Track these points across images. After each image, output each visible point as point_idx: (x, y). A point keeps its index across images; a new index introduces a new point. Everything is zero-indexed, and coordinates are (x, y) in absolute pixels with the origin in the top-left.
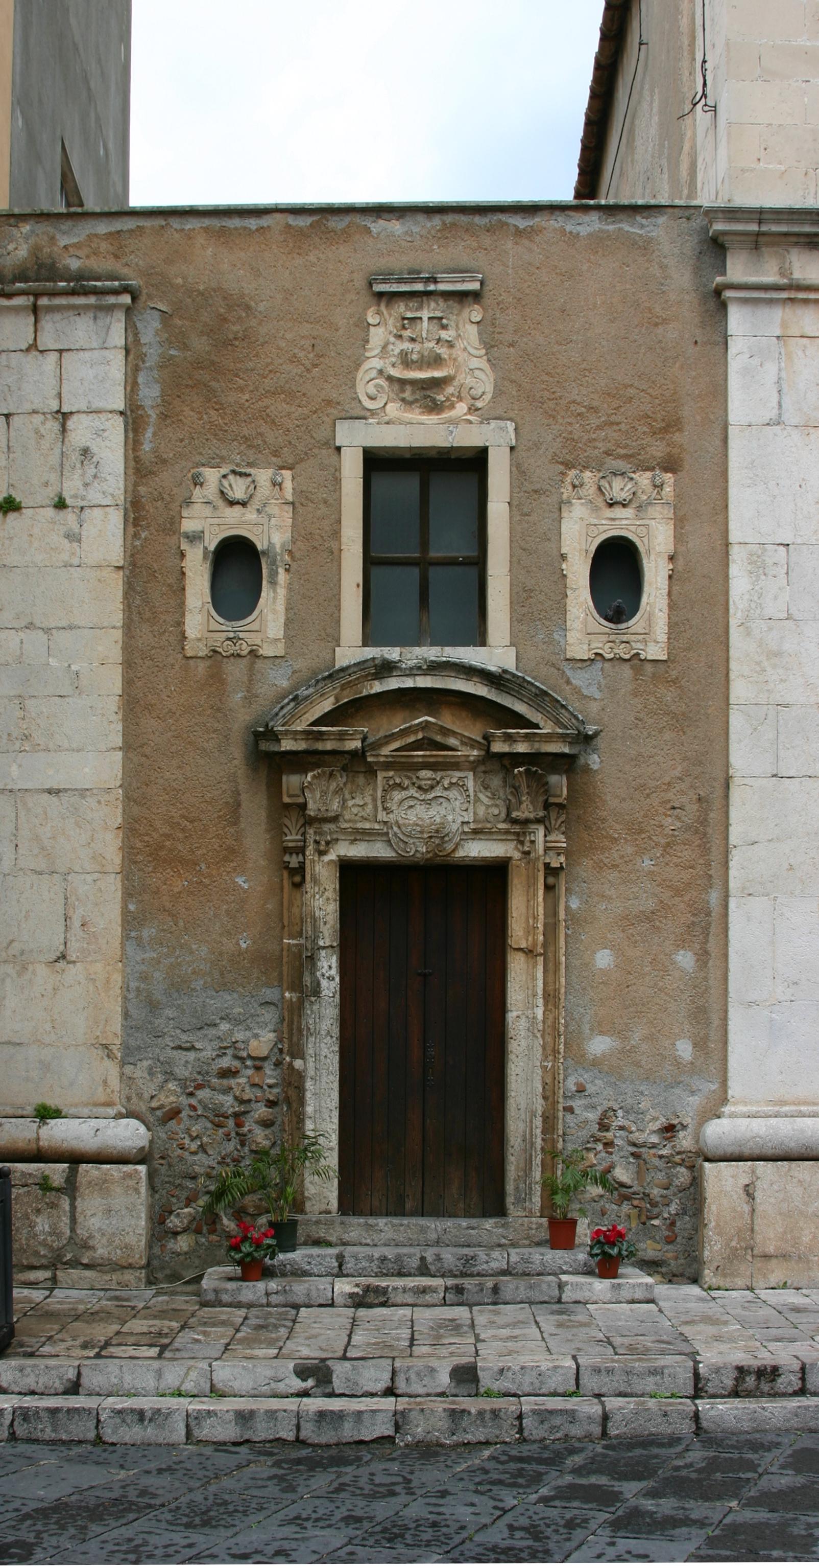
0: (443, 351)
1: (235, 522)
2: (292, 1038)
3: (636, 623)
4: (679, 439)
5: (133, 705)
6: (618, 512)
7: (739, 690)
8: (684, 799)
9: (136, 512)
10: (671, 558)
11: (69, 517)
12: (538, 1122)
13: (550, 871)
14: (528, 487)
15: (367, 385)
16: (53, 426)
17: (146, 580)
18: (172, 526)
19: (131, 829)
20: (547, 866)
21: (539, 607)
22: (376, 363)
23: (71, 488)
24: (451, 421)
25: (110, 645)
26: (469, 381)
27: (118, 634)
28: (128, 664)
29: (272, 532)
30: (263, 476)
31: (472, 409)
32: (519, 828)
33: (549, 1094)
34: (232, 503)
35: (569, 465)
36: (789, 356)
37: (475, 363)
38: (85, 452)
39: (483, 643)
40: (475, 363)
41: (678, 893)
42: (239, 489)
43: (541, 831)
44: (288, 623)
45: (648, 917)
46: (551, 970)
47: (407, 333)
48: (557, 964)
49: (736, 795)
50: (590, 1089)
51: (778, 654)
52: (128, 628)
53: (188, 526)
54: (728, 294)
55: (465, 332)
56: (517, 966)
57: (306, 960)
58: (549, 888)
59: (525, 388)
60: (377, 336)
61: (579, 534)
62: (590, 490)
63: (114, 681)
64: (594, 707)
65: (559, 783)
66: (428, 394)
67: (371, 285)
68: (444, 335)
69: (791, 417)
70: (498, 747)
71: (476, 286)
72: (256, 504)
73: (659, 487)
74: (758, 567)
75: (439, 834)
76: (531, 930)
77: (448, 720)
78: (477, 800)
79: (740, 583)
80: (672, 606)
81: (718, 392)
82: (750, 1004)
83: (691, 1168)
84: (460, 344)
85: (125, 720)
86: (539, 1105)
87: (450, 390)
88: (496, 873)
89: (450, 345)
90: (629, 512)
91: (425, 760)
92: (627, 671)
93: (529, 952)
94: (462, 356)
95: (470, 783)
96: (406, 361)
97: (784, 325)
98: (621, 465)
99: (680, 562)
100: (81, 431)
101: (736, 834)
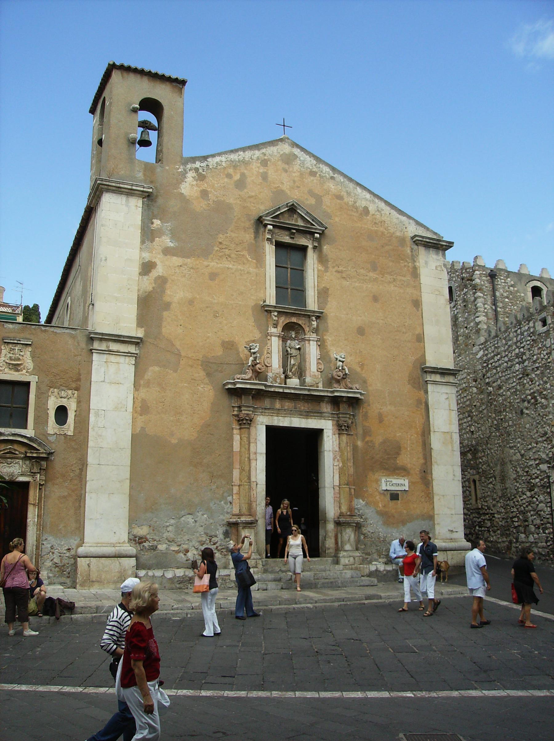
0: (21, 357)
6: (63, 399)
7: (91, 444)
8: (76, 469)
10: (75, 411)
12: (35, 547)
13: (40, 485)
14: (40, 391)
20: (40, 484)
21: (41, 420)
22: (3, 359)
24: (21, 374)
26: (27, 365)
31: (27, 372)
32: (33, 474)
33: (38, 540)
36: (108, 366)
37: (29, 361)
39: (26, 428)
40: (29, 361)
41: (73, 491)
43: (39, 475)
45: (65, 497)
47: (12, 352)
48: (41, 508)
49: (89, 468)
50: (49, 539)
51: (101, 436)
54: (93, 351)
55: (27, 354)
58: (40, 489)
60: (4, 352)
61: (52, 404)
62: (56, 394)
64: (54, 446)
65: (44, 463)
66: (16, 368)
67: (3, 340)
68: (21, 353)
69: (107, 381)
70: (28, 455)
71: (30, 343)
73: (74, 394)
74: (97, 415)
75: (12, 475)
76: (35, 499)
77: (16, 447)
78: (22, 466)
79: (92, 418)
81: (90, 373)
82: (91, 519)
83: (74, 559)
84: (25, 356)
86: (35, 543)
87: (22, 367)
89: (23, 356)
90: (66, 400)
92: (63, 437)
93: (34, 505)
94: (25, 359)
95: (21, 463)
96: (11, 359)
97: (107, 359)
98: (64, 388)
99: (78, 413)
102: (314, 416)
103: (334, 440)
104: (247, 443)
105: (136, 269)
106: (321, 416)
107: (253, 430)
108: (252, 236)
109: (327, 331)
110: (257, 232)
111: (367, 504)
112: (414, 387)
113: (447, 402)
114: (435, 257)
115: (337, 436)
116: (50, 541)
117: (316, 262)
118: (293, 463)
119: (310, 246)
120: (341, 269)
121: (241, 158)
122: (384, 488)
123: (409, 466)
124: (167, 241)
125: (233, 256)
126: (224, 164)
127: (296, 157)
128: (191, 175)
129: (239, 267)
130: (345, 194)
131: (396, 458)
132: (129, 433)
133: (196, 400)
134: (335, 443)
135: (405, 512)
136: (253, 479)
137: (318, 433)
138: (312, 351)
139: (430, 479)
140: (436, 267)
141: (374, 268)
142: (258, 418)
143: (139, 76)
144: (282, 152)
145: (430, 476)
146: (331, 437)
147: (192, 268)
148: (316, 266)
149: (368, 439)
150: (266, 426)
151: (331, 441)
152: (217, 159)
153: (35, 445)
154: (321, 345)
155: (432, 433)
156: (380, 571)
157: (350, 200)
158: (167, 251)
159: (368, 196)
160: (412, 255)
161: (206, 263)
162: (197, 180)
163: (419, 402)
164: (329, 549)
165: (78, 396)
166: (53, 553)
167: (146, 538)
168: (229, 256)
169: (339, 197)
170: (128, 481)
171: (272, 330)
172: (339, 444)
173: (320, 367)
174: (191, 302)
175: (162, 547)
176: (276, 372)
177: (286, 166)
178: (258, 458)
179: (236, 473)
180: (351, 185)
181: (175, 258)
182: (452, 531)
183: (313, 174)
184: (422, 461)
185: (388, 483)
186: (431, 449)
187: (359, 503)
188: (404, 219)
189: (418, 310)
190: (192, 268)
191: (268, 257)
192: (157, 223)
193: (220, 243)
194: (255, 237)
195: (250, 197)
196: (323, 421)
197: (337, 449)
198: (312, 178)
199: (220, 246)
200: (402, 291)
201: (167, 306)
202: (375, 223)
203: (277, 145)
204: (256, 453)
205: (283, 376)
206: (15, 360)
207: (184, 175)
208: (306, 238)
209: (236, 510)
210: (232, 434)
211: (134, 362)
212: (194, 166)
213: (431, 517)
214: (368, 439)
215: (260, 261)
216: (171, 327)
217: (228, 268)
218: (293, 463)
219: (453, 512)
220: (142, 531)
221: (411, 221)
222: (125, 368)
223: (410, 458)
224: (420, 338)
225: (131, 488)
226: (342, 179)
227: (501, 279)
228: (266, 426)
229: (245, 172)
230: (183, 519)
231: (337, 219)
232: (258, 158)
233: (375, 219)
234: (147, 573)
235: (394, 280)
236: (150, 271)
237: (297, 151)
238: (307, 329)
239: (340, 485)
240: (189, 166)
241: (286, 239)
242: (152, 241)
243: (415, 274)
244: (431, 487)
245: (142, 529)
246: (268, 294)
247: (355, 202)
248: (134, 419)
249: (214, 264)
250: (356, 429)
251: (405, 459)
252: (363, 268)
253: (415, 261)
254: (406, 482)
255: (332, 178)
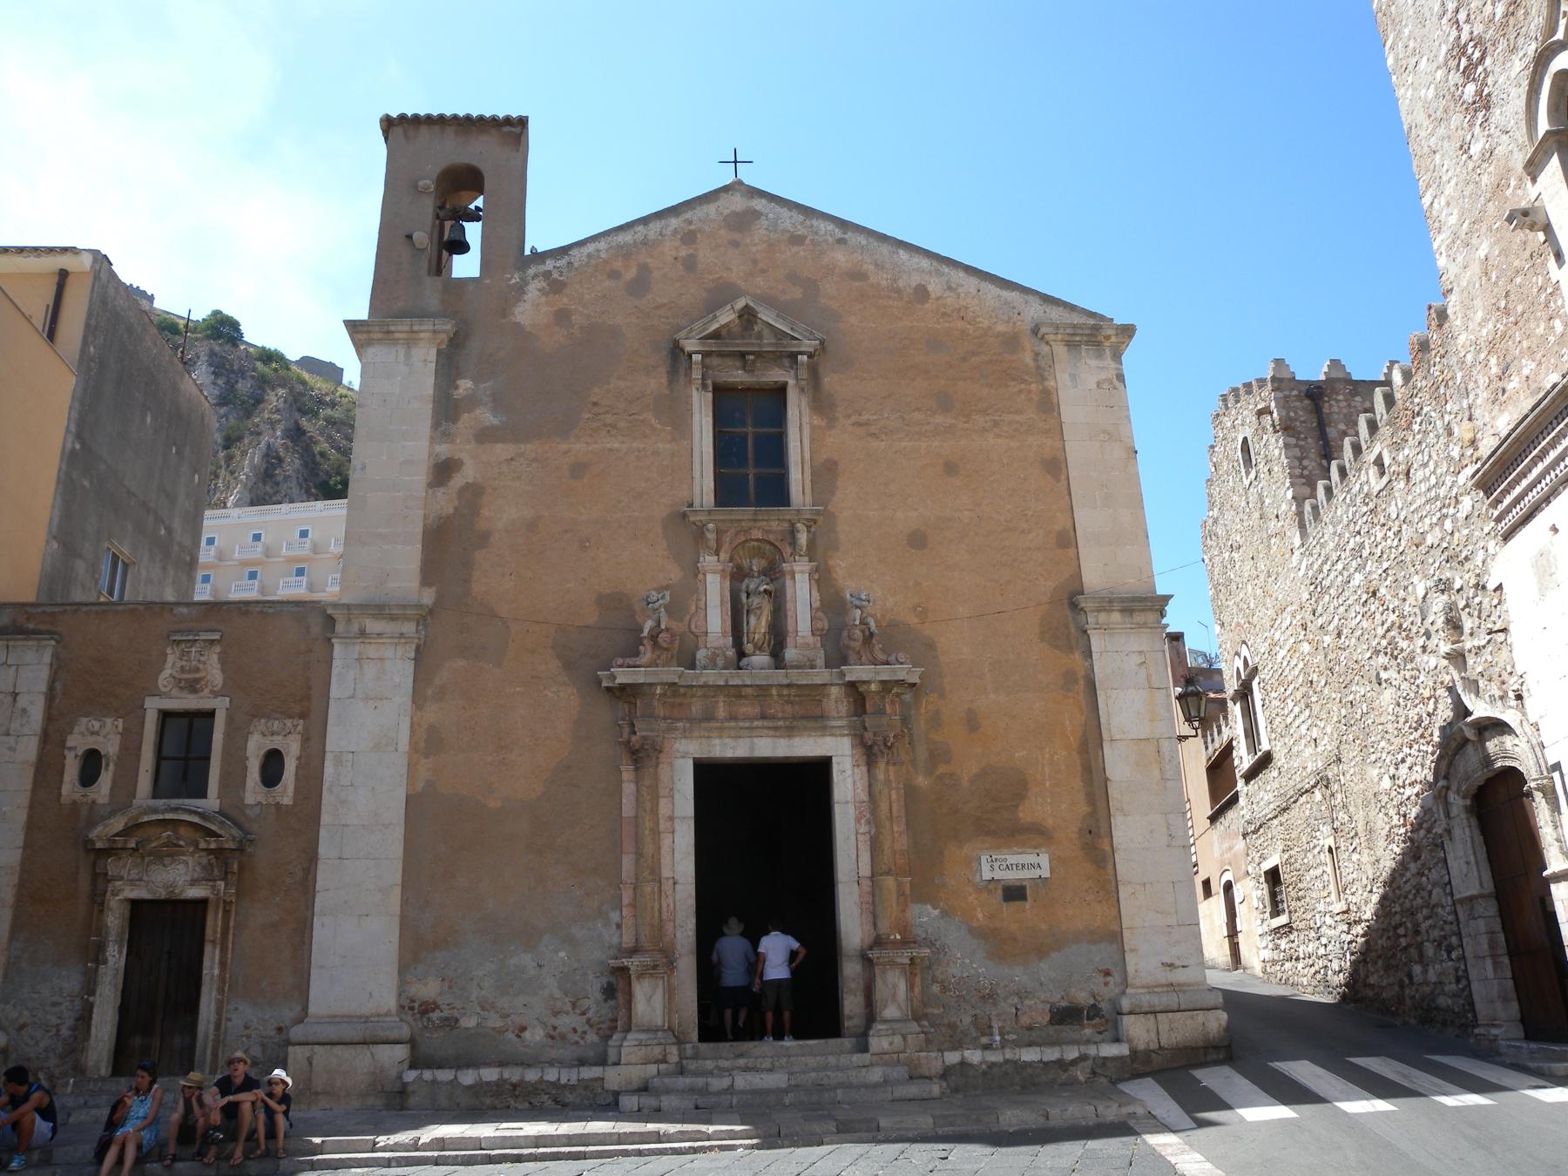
1: (91, 742)
2: (90, 987)
3: (279, 788)
4: (306, 704)
5: (31, 827)
7: (325, 818)
9: (45, 737)
11: (11, 740)
12: (212, 1027)
15: (164, 678)
16: (10, 699)
17: (46, 769)
18: (63, 744)
19: (21, 885)
23: (15, 726)
25: (24, 799)
27: (28, 794)
28: (31, 807)
29: (110, 747)
30: (109, 721)
33: (219, 1012)
34: (92, 733)
35: (254, 716)
38: (24, 711)
42: (97, 725)
44: (112, 789)
46: (224, 950)
49: (321, 867)
52: (34, 791)
53: (70, 743)
56: (208, 949)
57: (101, 947)
58: (227, 912)
59: (235, 682)
60: (170, 659)
63: (22, 816)
66: (193, 687)
71: (216, 636)
72: (103, 732)
73: (295, 726)
76: (215, 932)
77: (182, 831)
79: (329, 769)
80: (297, 779)
85: (27, 834)
88: (200, 906)
91: (170, 852)
93: (214, 942)
100: (23, 701)
101: (319, 886)
102: (805, 728)
103: (857, 777)
104: (651, 795)
105: (419, 477)
106: (824, 728)
107: (664, 771)
108: (664, 381)
109: (837, 549)
110: (673, 372)
111: (945, 914)
112: (1057, 647)
113: (1143, 672)
114: (1093, 363)
115: (864, 769)
116: (243, 1014)
117: (806, 410)
118: (765, 833)
119: (791, 382)
120: (865, 417)
121: (639, 237)
122: (987, 875)
123: (1050, 821)
124: (486, 416)
125: (622, 424)
126: (603, 255)
127: (756, 215)
128: (533, 289)
129: (635, 445)
130: (871, 267)
131: (1017, 807)
132: (401, 794)
133: (544, 718)
134: (859, 784)
135: (1044, 927)
136: (666, 873)
137: (821, 768)
138: (801, 593)
139: (1108, 848)
140: (1098, 384)
141: (945, 403)
142: (677, 745)
143: (436, 128)
144: (726, 212)
145: (1107, 841)
146: (849, 772)
147: (535, 460)
148: (806, 419)
149: (941, 769)
150: (695, 759)
151: (850, 781)
152: (591, 248)
153: (214, 828)
154: (822, 578)
155: (1106, 746)
156: (971, 1065)
157: (883, 280)
158: (485, 436)
159: (925, 263)
160: (1038, 367)
161: (564, 447)
162: (546, 294)
163: (1069, 678)
164: (850, 1018)
165: (306, 729)
166: (248, 1037)
167: (435, 1003)
168: (614, 426)
169: (857, 275)
170: (398, 890)
171: (709, 560)
172: (870, 785)
173: (820, 625)
174: (532, 526)
175: (469, 1022)
176: (716, 644)
177: (736, 236)
178: (677, 828)
179: (627, 862)
180: (885, 249)
181: (499, 446)
182: (1171, 965)
183: (797, 240)
184: (1084, 809)
185: (996, 865)
186: (1107, 779)
187: (925, 916)
188: (1006, 294)
189: (1058, 481)
190: (535, 460)
191: (696, 417)
192: (465, 385)
193: (595, 404)
194: (670, 382)
195: (658, 307)
196: (828, 739)
197: (864, 796)
198: (795, 249)
199: (595, 410)
200: (1014, 444)
201: (484, 539)
202: (944, 314)
203: (717, 200)
204: (671, 819)
205: (731, 653)
206: (189, 672)
207: (521, 289)
208: (781, 366)
209: (628, 940)
210: (620, 783)
211: (412, 655)
212: (542, 268)
213: (1115, 937)
214: (941, 769)
215: (680, 425)
216: (492, 580)
217: (611, 450)
218: (765, 833)
219: (1173, 920)
220: (428, 989)
221: (1030, 298)
222: (398, 669)
223: (1054, 803)
224: (1067, 540)
225: (405, 902)
226: (862, 240)
227: (1338, 401)
228: (695, 759)
229: (649, 260)
230: (512, 962)
231: (853, 320)
232: (675, 232)
233: (944, 306)
234: (420, 1077)
235: (996, 424)
236: (450, 477)
237: (759, 204)
238: (787, 550)
239: (873, 875)
240: (531, 271)
241: (738, 376)
242: (454, 419)
243: (1048, 404)
244: (1110, 866)
245: (426, 985)
246: (697, 490)
247: (895, 281)
248: (412, 767)
249: (579, 447)
250: (913, 750)
251: (1036, 808)
252: (918, 409)
253: (1043, 379)
254: (1044, 860)
255: (841, 241)
